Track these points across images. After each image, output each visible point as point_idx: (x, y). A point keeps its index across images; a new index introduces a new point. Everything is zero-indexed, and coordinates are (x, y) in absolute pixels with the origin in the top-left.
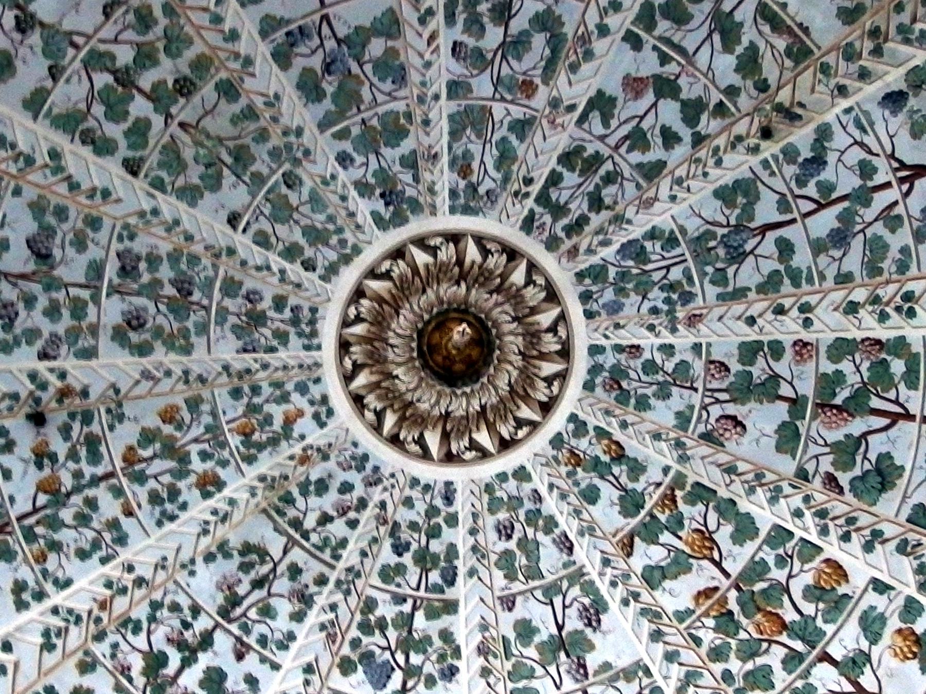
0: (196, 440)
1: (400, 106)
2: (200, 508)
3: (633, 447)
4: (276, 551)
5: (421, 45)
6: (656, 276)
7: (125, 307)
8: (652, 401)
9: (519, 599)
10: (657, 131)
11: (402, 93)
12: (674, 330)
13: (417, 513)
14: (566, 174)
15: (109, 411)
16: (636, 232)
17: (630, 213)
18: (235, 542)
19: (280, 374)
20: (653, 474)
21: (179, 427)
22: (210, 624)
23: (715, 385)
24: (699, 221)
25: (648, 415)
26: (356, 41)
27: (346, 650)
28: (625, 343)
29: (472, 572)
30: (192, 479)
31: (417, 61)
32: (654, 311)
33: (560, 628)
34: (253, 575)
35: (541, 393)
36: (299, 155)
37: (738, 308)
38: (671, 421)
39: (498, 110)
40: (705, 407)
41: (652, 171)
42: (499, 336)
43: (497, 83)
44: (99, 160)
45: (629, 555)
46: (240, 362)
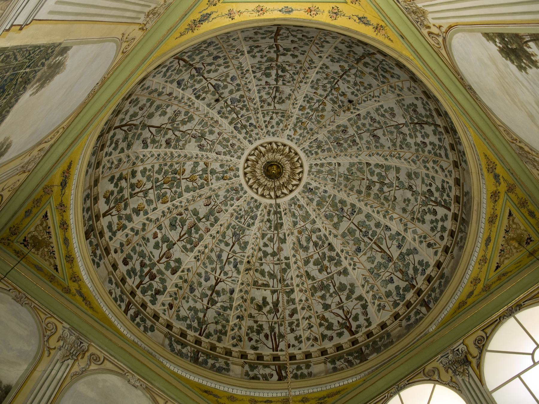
0: (312, 115)
1: (322, 210)
2: (300, 102)
3: (222, 182)
5: (327, 226)
6: (246, 217)
7: (349, 134)
8: (226, 193)
9: (218, 136)
11: (324, 213)
12: (234, 210)
13: (253, 134)
15: (336, 110)
16: (257, 222)
17: (261, 224)
18: (287, 101)
19: (305, 139)
20: (214, 181)
21: (318, 115)
23: (217, 208)
25: (225, 190)
26: (341, 218)
27: (245, 99)
29: (232, 132)
30: (307, 107)
32: (241, 210)
33: (205, 139)
34: (278, 98)
35: (249, 176)
37: (226, 225)
38: (219, 193)
39: (302, 224)
41: (263, 236)
43: (306, 229)
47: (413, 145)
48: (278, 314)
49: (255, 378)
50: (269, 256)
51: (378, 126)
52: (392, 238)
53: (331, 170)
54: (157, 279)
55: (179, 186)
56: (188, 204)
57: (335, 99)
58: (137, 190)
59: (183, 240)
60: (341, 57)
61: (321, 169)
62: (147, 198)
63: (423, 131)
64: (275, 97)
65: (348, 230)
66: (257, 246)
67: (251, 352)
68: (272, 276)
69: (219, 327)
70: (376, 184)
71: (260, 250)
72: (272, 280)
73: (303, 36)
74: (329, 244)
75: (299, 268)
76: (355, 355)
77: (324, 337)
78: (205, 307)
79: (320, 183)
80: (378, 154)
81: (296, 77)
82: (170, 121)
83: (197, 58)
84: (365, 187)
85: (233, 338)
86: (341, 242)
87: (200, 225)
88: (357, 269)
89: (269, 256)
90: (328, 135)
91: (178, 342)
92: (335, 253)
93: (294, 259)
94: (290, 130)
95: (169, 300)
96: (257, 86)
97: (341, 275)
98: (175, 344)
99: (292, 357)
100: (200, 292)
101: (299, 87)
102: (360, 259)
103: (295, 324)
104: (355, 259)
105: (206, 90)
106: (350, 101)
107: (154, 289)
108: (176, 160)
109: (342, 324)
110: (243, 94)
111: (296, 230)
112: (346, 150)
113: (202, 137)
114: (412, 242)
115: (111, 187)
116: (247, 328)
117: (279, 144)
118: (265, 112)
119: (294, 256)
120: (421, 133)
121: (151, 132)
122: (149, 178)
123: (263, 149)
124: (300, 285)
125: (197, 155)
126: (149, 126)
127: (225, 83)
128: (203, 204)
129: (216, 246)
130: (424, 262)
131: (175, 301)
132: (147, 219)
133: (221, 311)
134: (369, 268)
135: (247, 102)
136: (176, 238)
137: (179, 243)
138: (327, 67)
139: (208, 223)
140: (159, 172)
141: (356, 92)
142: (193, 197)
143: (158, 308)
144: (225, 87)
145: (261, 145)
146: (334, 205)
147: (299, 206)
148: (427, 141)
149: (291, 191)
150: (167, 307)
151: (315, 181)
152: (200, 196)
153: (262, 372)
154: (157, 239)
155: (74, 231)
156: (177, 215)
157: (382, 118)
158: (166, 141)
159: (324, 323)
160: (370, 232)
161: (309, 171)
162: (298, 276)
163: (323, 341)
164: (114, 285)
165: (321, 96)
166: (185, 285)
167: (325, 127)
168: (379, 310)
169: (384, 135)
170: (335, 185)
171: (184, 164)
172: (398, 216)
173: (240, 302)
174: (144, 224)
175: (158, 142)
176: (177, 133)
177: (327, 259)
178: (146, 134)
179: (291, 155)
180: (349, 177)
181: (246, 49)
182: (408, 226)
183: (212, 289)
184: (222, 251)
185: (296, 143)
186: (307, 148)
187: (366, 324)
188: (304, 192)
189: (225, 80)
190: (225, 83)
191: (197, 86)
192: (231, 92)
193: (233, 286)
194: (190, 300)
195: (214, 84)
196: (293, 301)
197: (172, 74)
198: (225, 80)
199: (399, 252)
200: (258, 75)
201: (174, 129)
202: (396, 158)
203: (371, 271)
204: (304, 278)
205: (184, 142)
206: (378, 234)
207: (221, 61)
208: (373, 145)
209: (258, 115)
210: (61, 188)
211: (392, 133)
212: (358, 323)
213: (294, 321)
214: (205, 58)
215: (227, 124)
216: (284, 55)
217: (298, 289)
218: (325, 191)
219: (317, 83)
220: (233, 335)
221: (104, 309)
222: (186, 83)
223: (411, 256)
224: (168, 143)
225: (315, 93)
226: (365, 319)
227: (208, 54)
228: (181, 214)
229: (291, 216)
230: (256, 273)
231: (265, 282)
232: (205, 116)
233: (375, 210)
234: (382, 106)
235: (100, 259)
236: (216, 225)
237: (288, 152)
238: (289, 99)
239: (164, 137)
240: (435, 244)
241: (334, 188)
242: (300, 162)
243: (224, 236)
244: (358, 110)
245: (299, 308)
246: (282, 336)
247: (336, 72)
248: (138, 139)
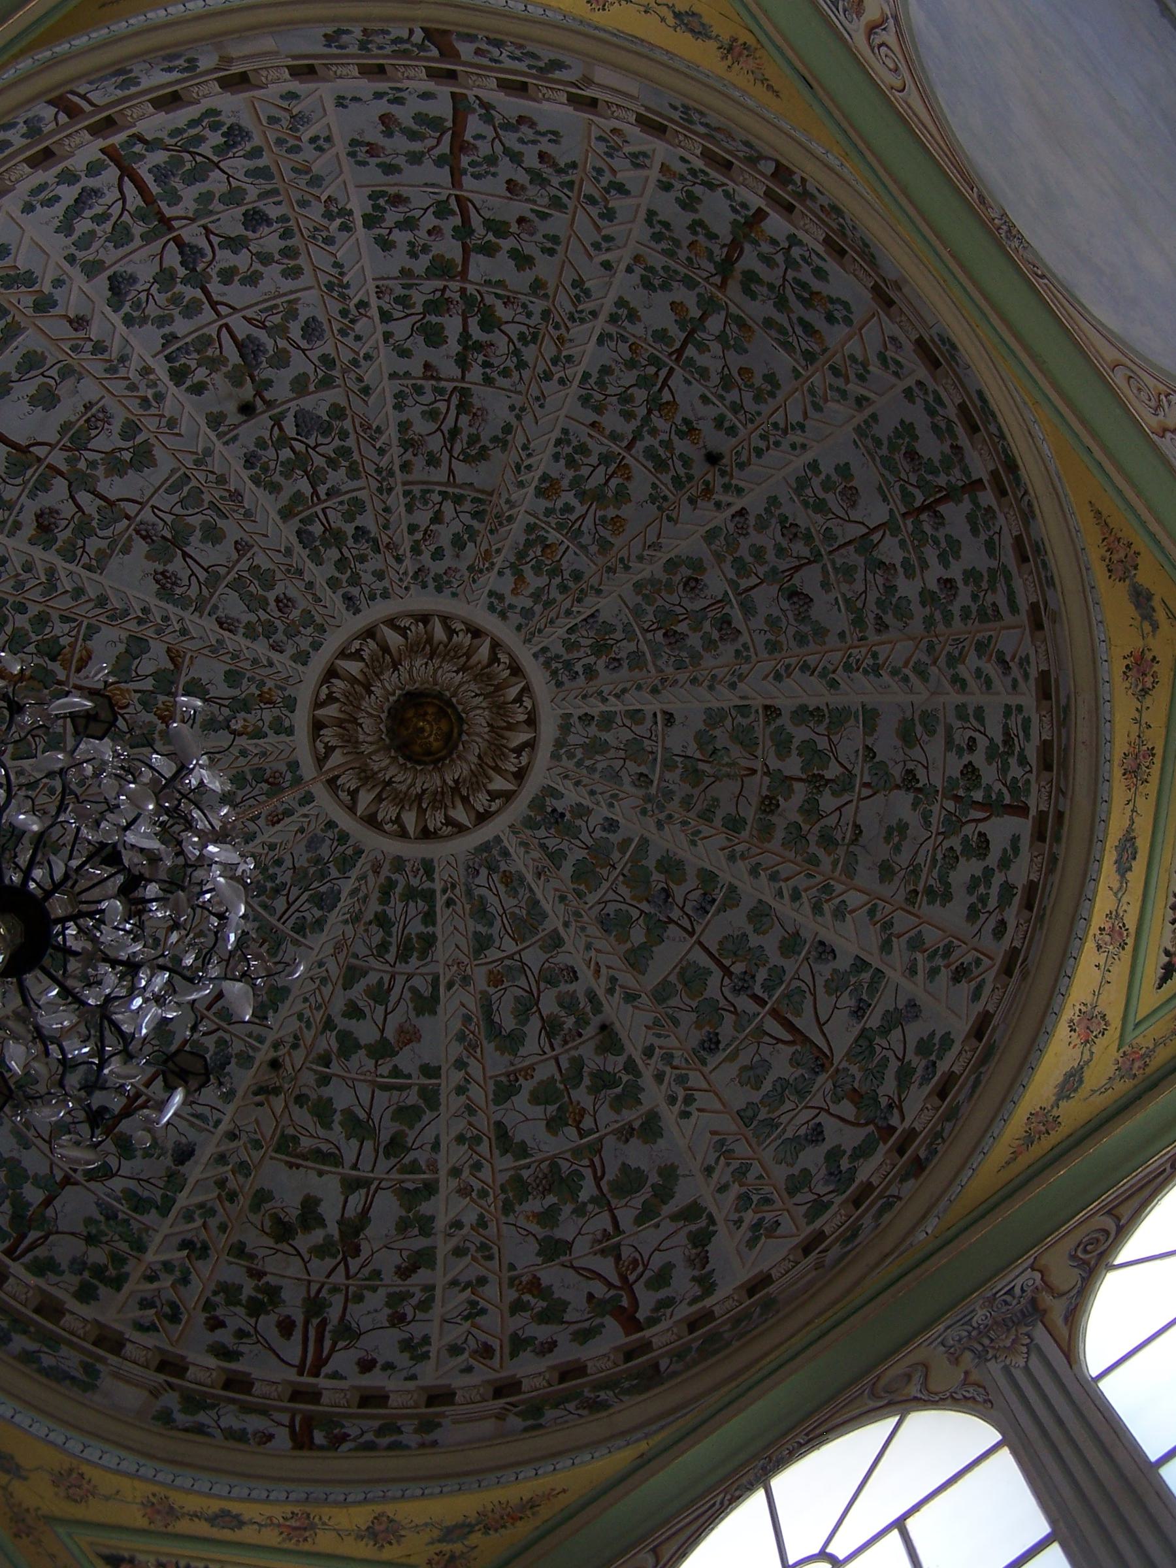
0: (584, 517)
1: (592, 899)
2: (543, 463)
4: (458, 466)
5: (603, 959)
6: (295, 892)
9: (235, 556)
10: (367, 1010)
13: (366, 572)
14: (422, 929)
15: (665, 498)
16: (334, 917)
18: (496, 454)
19: (553, 615)
21: (603, 519)
22: (468, 376)
26: (657, 929)
27: (347, 424)
28: (287, 820)
29: (289, 552)
30: (565, 484)
31: (598, 944)
32: (279, 862)
33: (185, 555)
34: (464, 436)
35: (329, 735)
36: (649, 806)
39: (510, 946)
41: (352, 975)
42: (394, 759)
44: (799, 702)
45: (169, 650)
46: (591, 603)
47: (915, 607)
49: (200, 1429)
50: (363, 1052)
51: (805, 552)
52: (836, 985)
53: (637, 740)
57: (661, 451)
60: (671, 263)
61: (604, 736)
63: (941, 535)
64: (455, 432)
65: (681, 975)
66: (318, 1008)
68: (358, 1127)
70: (797, 786)
71: (329, 1024)
72: (354, 1143)
73: (542, 156)
74: (603, 1027)
75: (471, 1110)
76: (626, 1385)
77: (518, 1344)
79: (592, 793)
80: (805, 668)
81: (529, 353)
83: (189, 195)
84: (755, 801)
86: (648, 1018)
88: (696, 1114)
89: (363, 1052)
90: (634, 600)
92: (621, 1060)
93: (457, 1077)
94: (501, 573)
96: (393, 376)
97: (633, 1140)
99: (372, 1399)
101: (541, 399)
102: (712, 1077)
103: (414, 1301)
104: (695, 1079)
105: (210, 352)
106: (713, 459)
108: (63, 603)
110: (344, 403)
111: (484, 969)
112: (696, 658)
113: (174, 543)
114: (905, 983)
116: (212, 1286)
117: (458, 626)
118: (417, 490)
119: (460, 1064)
120: (936, 542)
123: (394, 639)
124: (466, 1173)
125: (145, 610)
127: (282, 343)
130: (936, 1040)
133: (123, 1209)
134: (739, 1104)
135: (353, 436)
138: (633, 316)
141: (730, 415)
144: (281, 360)
145: (391, 623)
146: (637, 878)
147: (507, 878)
148: (955, 572)
149: (482, 818)
151: (577, 784)
153: (231, 1419)
157: (819, 518)
158: (39, 516)
159: (533, 1301)
160: (762, 974)
161: (559, 743)
162: (460, 1139)
163: (514, 1354)
165: (614, 437)
167: (627, 568)
168: (752, 1243)
169: (826, 585)
170: (648, 799)
171: (92, 631)
172: (865, 898)
176: (84, 497)
177: (587, 1081)
179: (497, 675)
180: (702, 766)
181: (358, 205)
182: (897, 929)
185: (519, 628)
186: (558, 649)
187: (697, 1290)
188: (529, 823)
189: (280, 330)
190: (282, 343)
191: (181, 326)
192: (300, 385)
195: (240, 337)
196: (426, 1225)
197: (92, 233)
198: (280, 330)
199: (856, 1031)
200: (401, 329)
201: (79, 481)
202: (866, 672)
203: (745, 1117)
204: (484, 1148)
205: (104, 544)
206: (787, 978)
207: (269, 240)
208: (791, 631)
209: (391, 501)
211: (848, 572)
212: (663, 1293)
213: (416, 1290)
214: (216, 206)
215: (274, 515)
216: (489, 250)
217: (454, 1183)
218: (611, 825)
219: (601, 384)
220: (148, 1295)
222: (143, 296)
223: (896, 1034)
224: (45, 525)
225: (593, 425)
226: (694, 1279)
227: (224, 188)
229: (472, 916)
230: (295, 1109)
231: (325, 1147)
232: (197, 462)
233: (787, 889)
234: (814, 466)
237: (485, 661)
238: (505, 444)
239: (32, 496)
240: (978, 962)
241: (644, 812)
242: (528, 703)
244: (739, 491)
245: (443, 1248)
246: (348, 1332)
247: (661, 336)
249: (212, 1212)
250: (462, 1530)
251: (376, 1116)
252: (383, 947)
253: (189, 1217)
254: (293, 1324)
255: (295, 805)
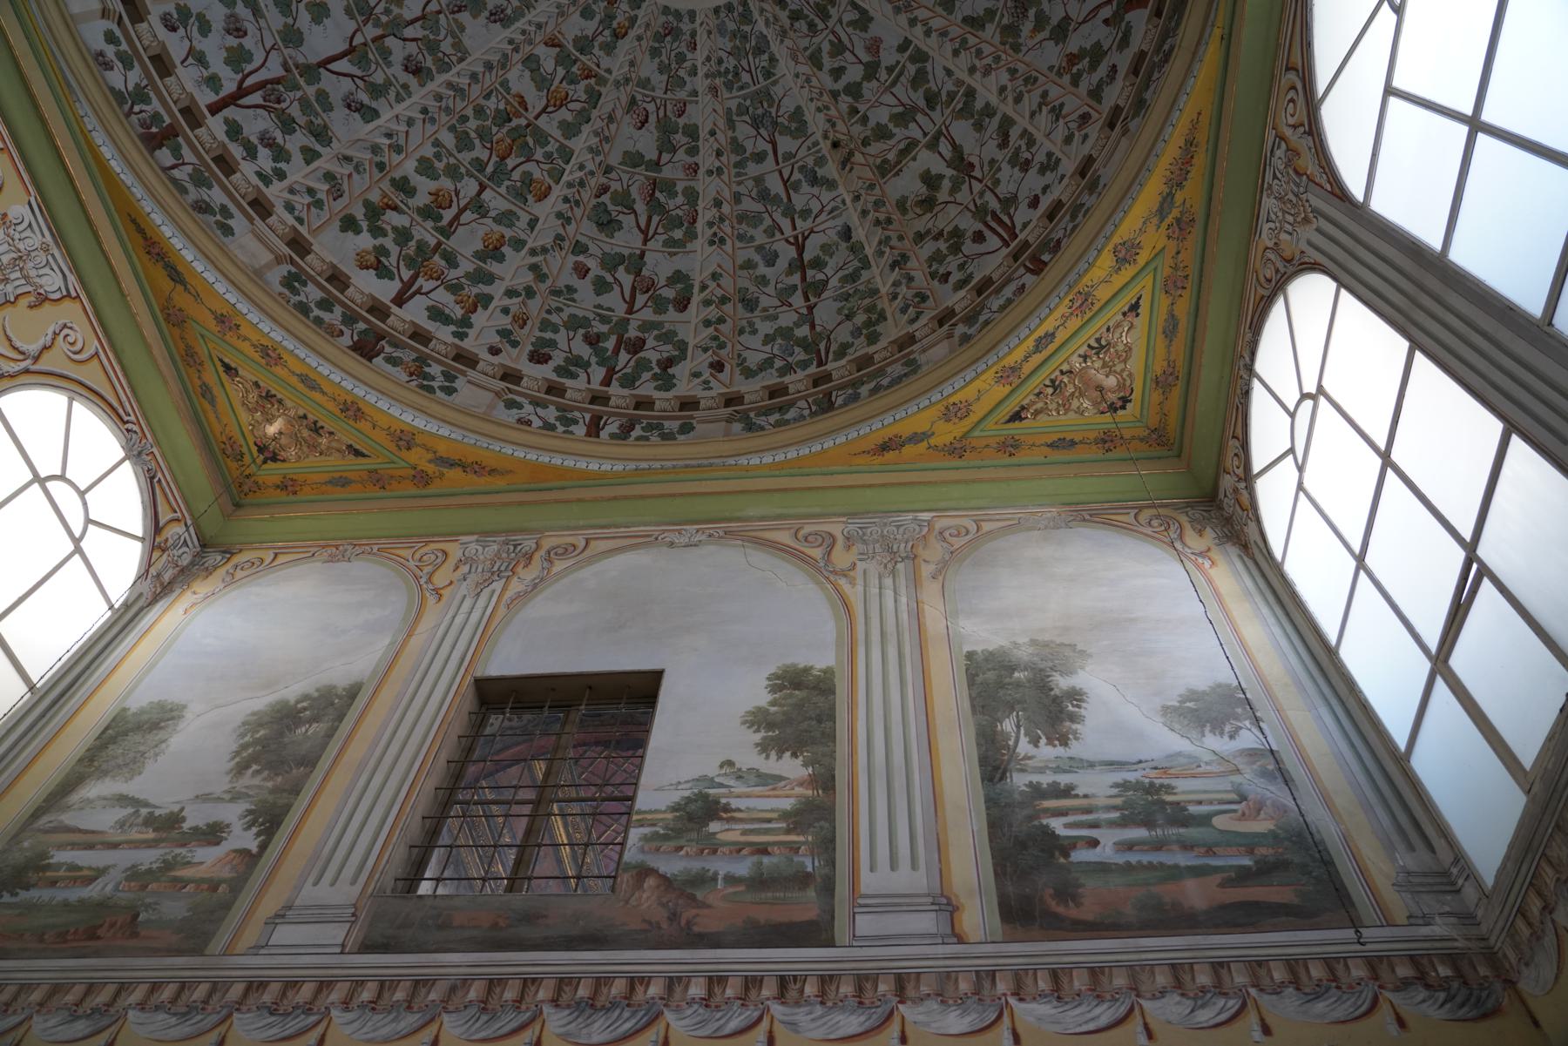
3: (624, 46)
6: (744, 63)
8: (657, 60)
12: (707, 76)
16: (774, 47)
17: (788, 42)
20: (606, 62)
23: (669, 107)
24: (780, 94)
25: (647, 57)
32: (720, 61)
37: (721, 123)
38: (644, 73)
40: (653, 99)
48: (977, 173)
50: (865, 84)
54: (650, 343)
55: (542, 138)
56: (601, 158)
58: (448, 215)
59: (655, 233)
62: (493, 214)
67: (958, 299)
68: (905, 116)
69: (860, 318)
71: (835, 95)
75: (944, 34)
78: (804, 311)
82: (360, 19)
85: (904, 310)
87: (667, 173)
89: (865, 84)
91: (767, 412)
93: (919, 30)
95: (708, 357)
98: (761, 421)
100: (773, 293)
103: (1024, 148)
107: (654, 365)
108: (476, 90)
109: (1116, 14)
115: (365, 241)
119: (913, 22)
121: (345, 75)
122: (453, 172)
124: (978, 63)
125: (511, 42)
126: (325, 63)
128: (632, 129)
129: (739, 183)
131: (723, 352)
132: (533, 252)
133: (849, 288)
136: (636, 241)
137: (651, 245)
139: (680, 154)
140: (464, 142)
142: (597, 134)
143: (685, 386)
150: (706, 375)
152: (611, 119)
153: (996, 303)
154: (591, 275)
155: (302, 352)
156: (597, 196)
158: (406, 69)
162: (956, 53)
164: (528, 408)
166: (728, 308)
173: (879, 233)
174: (534, 268)
175: (388, 83)
178: (336, 88)
183: (799, 265)
184: (759, 180)
193: (839, 222)
194: (759, 324)
196: (989, 111)
204: (972, 40)
210: (180, 288)
217: (978, 75)
221: (520, 454)
224: (416, 70)
228: (604, 189)
231: (902, 146)
235: (449, 377)
236: (700, 143)
239: (389, 64)
243: (737, 147)
245: (1008, 109)
246: (1009, 202)
248: (328, 108)
249: (888, 238)
250: (1167, 200)
251: (905, 100)
252: (812, 25)
253: (881, 254)
254: (980, 232)
255: (691, 26)
